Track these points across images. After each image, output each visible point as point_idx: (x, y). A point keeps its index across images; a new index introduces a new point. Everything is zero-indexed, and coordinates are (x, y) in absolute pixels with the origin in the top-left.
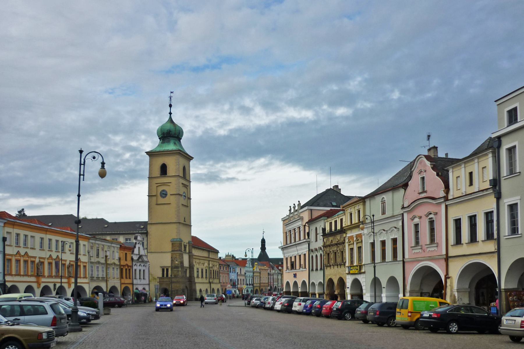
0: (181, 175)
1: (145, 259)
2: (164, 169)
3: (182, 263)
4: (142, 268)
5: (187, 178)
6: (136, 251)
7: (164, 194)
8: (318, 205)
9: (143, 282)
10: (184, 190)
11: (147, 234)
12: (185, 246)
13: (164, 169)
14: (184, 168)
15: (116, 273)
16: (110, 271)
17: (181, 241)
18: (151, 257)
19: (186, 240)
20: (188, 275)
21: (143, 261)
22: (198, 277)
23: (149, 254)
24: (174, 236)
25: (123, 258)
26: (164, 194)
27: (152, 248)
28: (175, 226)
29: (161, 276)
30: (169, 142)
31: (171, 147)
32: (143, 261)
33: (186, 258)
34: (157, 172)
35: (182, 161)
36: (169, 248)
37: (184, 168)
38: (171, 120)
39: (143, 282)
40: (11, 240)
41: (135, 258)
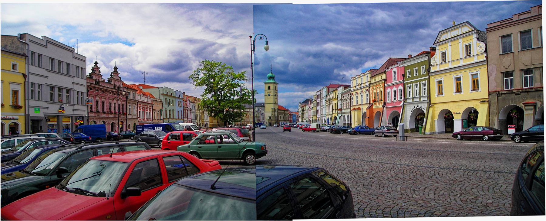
0: (275, 89)
1: (264, 114)
2: (269, 88)
3: (275, 115)
4: (263, 117)
5: (277, 90)
6: (261, 112)
7: (269, 95)
8: (304, 103)
9: (263, 121)
10: (276, 93)
11: (264, 107)
12: (276, 110)
13: (269, 88)
14: (275, 87)
17: (274, 108)
18: (266, 114)
19: (276, 107)
20: (277, 118)
21: (263, 115)
22: (280, 119)
23: (265, 113)
24: (273, 107)
25: (257, 114)
26: (269, 95)
27: (266, 111)
28: (273, 104)
29: (268, 119)
30: (271, 79)
31: (271, 81)
32: (263, 115)
33: (276, 113)
34: (267, 88)
35: (275, 85)
36: (271, 110)
37: (275, 87)
39: (263, 121)
41: (261, 114)
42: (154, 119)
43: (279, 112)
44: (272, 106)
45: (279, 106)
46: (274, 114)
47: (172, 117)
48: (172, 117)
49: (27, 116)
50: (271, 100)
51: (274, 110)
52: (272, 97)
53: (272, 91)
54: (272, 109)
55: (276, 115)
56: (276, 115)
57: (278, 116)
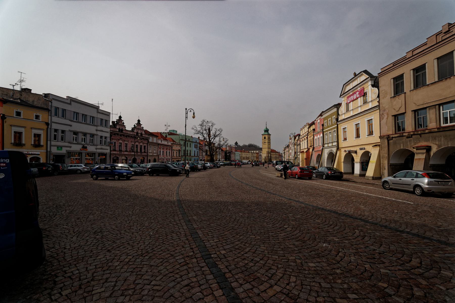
2: (265, 138)
7: (265, 143)
13: (265, 138)
14: (269, 137)
15: (256, 158)
16: (255, 158)
19: (270, 151)
24: (267, 151)
26: (265, 143)
31: (266, 133)
37: (269, 137)
38: (267, 128)
40: (241, 154)
42: (173, 155)
43: (272, 153)
44: (267, 150)
45: (271, 150)
46: (268, 155)
47: (189, 155)
48: (189, 155)
49: (48, 153)
50: (266, 146)
51: (268, 153)
52: (267, 144)
53: (267, 140)
54: (267, 152)
55: (270, 156)
56: (270, 156)
57: (271, 157)
